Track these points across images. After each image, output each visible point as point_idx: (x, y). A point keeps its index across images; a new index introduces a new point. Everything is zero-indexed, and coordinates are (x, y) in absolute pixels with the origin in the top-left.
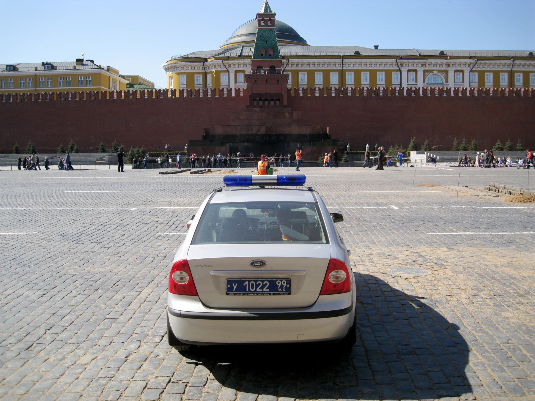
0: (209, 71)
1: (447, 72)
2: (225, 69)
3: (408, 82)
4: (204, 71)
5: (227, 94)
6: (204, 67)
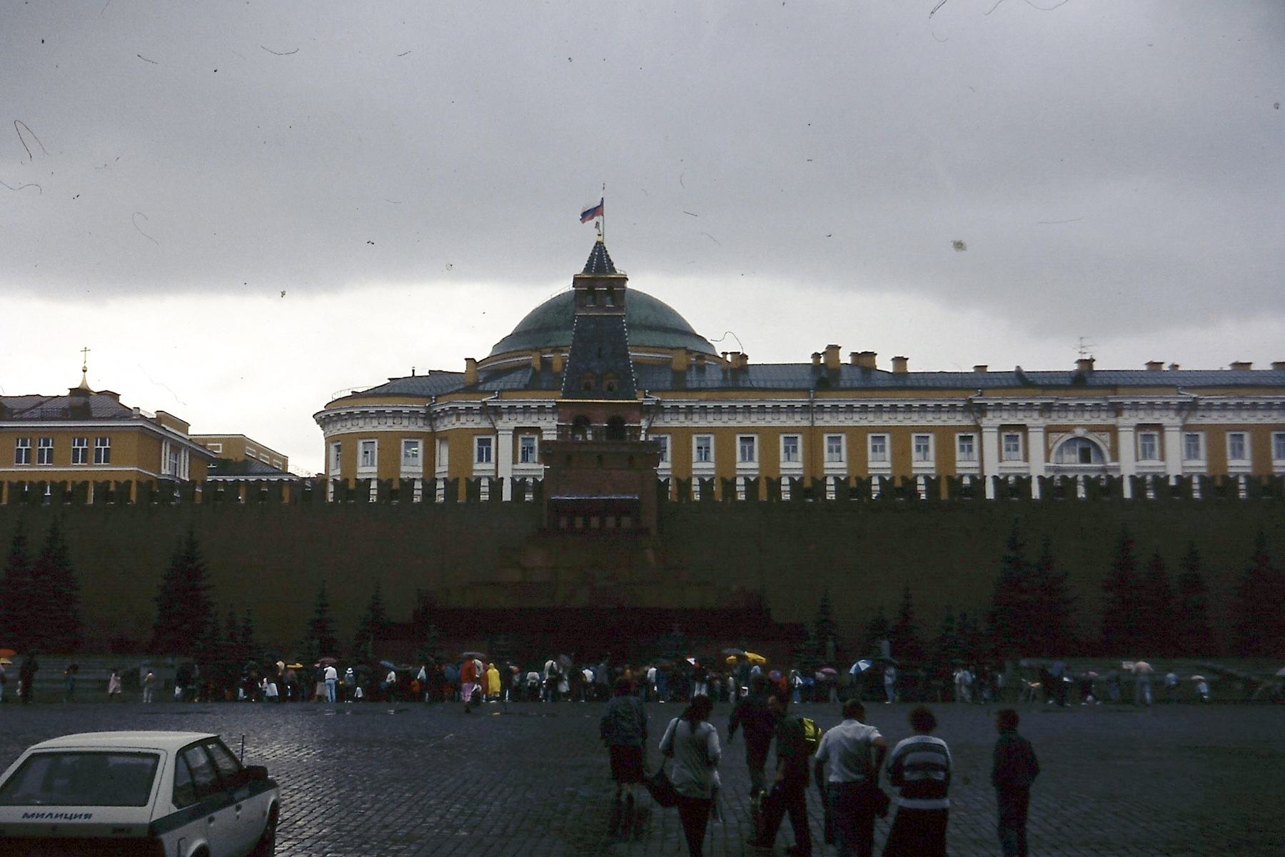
0: (442, 428)
1: (1113, 431)
3: (1001, 460)
4: (427, 429)
5: (490, 493)
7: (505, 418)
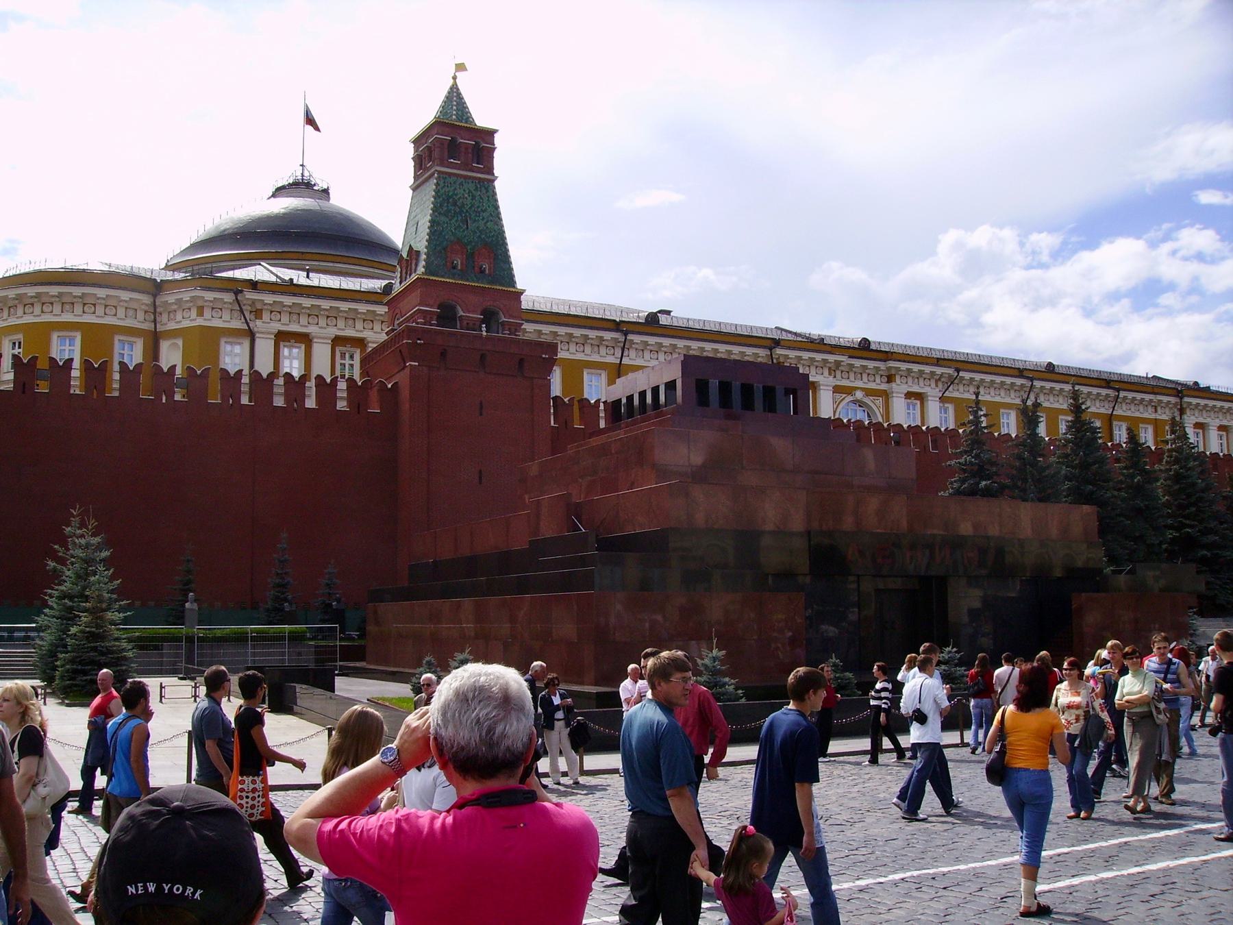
0: (172, 326)
1: (886, 395)
2: (238, 324)
4: (148, 326)
6: (154, 311)
7: (266, 316)
